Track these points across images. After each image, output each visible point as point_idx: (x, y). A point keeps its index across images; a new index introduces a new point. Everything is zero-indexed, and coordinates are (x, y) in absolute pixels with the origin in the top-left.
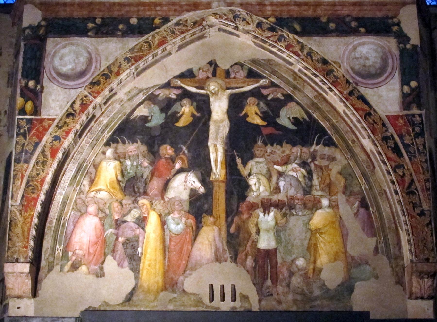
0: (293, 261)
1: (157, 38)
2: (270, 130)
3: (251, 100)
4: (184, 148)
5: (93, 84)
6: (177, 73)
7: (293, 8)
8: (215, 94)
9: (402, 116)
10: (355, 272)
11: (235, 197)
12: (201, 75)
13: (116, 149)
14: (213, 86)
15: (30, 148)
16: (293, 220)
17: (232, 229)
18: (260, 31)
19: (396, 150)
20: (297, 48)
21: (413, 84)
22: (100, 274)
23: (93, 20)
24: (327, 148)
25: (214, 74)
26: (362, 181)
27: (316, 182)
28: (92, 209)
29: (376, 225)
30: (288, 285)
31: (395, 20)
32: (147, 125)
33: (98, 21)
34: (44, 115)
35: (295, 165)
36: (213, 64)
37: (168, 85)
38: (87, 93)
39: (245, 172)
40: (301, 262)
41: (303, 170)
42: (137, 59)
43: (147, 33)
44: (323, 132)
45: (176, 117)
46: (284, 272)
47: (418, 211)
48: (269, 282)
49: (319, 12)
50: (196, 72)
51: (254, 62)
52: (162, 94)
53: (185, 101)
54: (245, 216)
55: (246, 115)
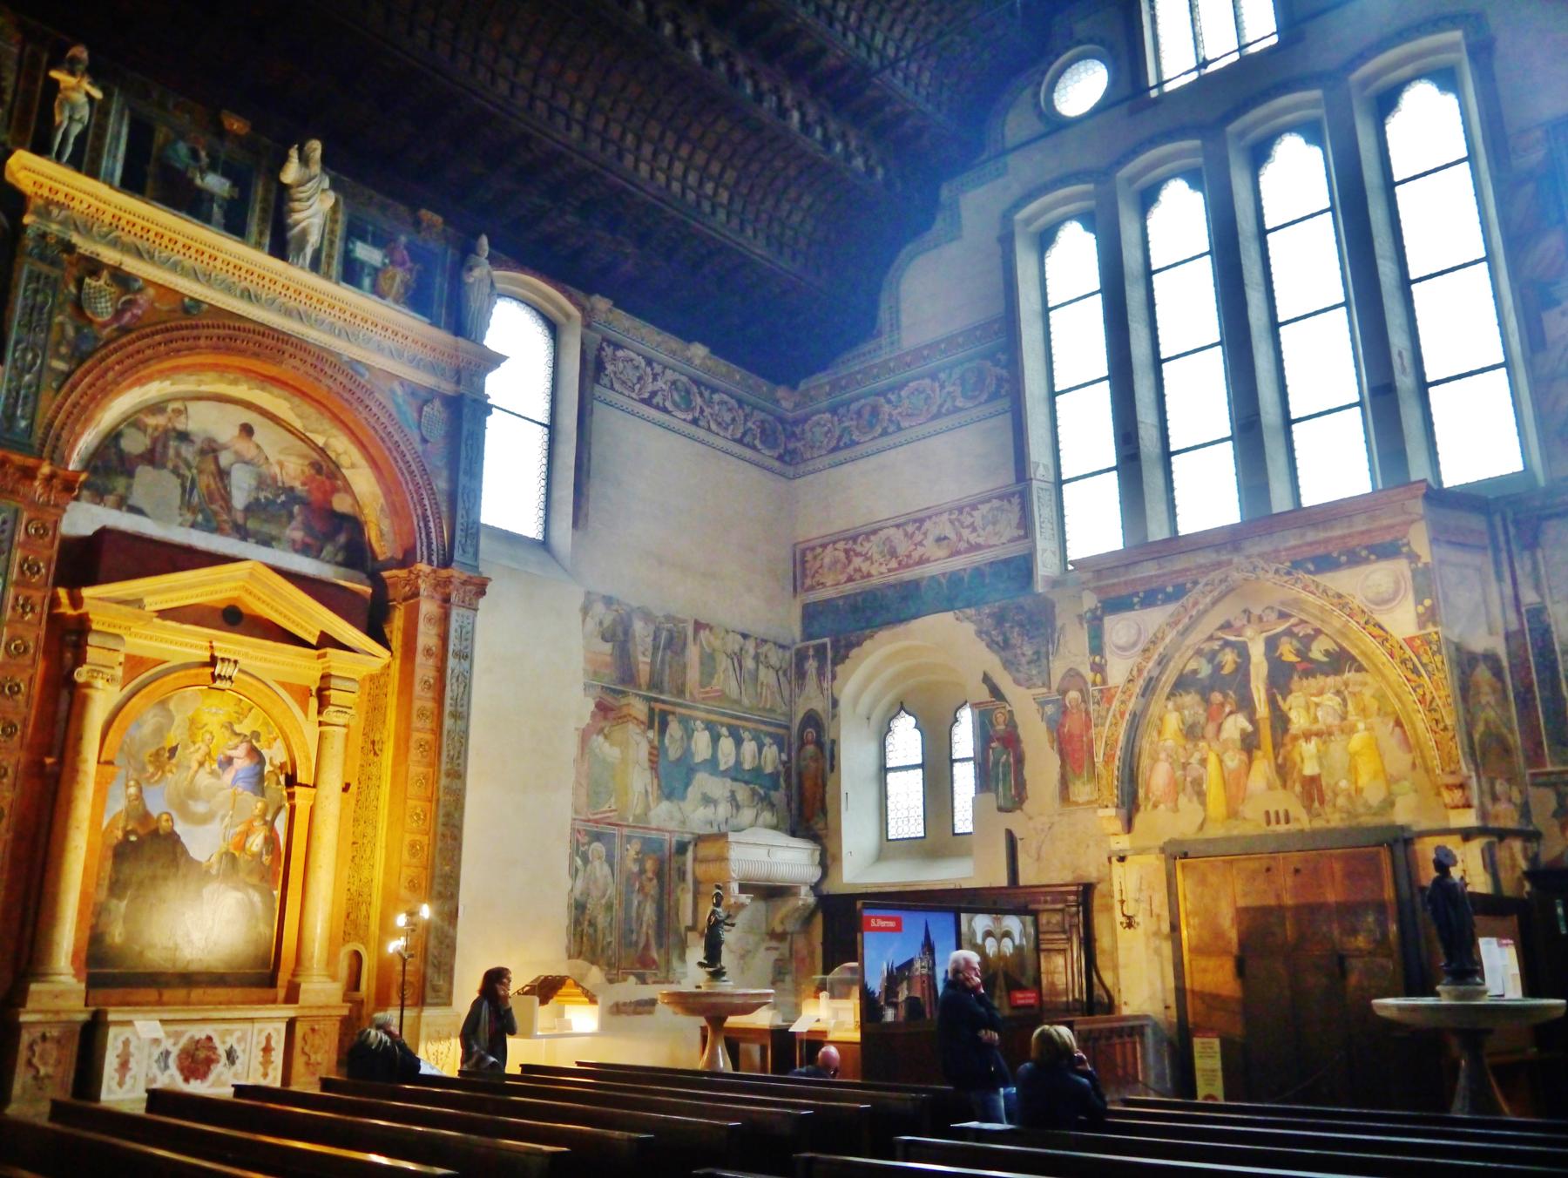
0: (1336, 784)
1: (1191, 600)
2: (1305, 665)
3: (1285, 639)
4: (1231, 693)
5: (1145, 651)
6: (1218, 624)
7: (1305, 549)
8: (1252, 639)
9: (1418, 637)
10: (1395, 788)
11: (1280, 731)
12: (1237, 624)
13: (1175, 702)
14: (1249, 632)
15: (1103, 713)
16: (1332, 746)
17: (1280, 760)
18: (1277, 577)
19: (1415, 671)
20: (1313, 588)
21: (1428, 602)
22: (1176, 809)
23: (1136, 594)
24: (1358, 675)
25: (1249, 621)
26: (1394, 701)
27: (1350, 707)
28: (1163, 756)
29: (1412, 741)
30: (1334, 805)
31: (1405, 541)
32: (1199, 676)
33: (1141, 595)
34: (1111, 682)
35: (1329, 695)
36: (1247, 612)
37: (1211, 638)
38: (1139, 660)
39: (1285, 707)
40: (1343, 784)
41: (1338, 699)
42: (1176, 623)
43: (1183, 596)
44: (1353, 659)
45: (1220, 667)
46: (1329, 795)
47: (1441, 726)
48: (1316, 804)
49: (1330, 548)
50: (1233, 622)
51: (1283, 603)
52: (1207, 647)
53: (1228, 650)
54: (1289, 747)
55: (1281, 655)
